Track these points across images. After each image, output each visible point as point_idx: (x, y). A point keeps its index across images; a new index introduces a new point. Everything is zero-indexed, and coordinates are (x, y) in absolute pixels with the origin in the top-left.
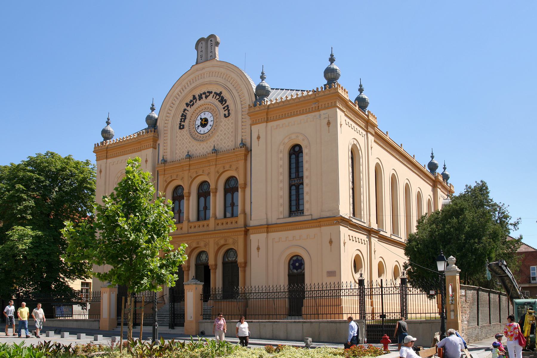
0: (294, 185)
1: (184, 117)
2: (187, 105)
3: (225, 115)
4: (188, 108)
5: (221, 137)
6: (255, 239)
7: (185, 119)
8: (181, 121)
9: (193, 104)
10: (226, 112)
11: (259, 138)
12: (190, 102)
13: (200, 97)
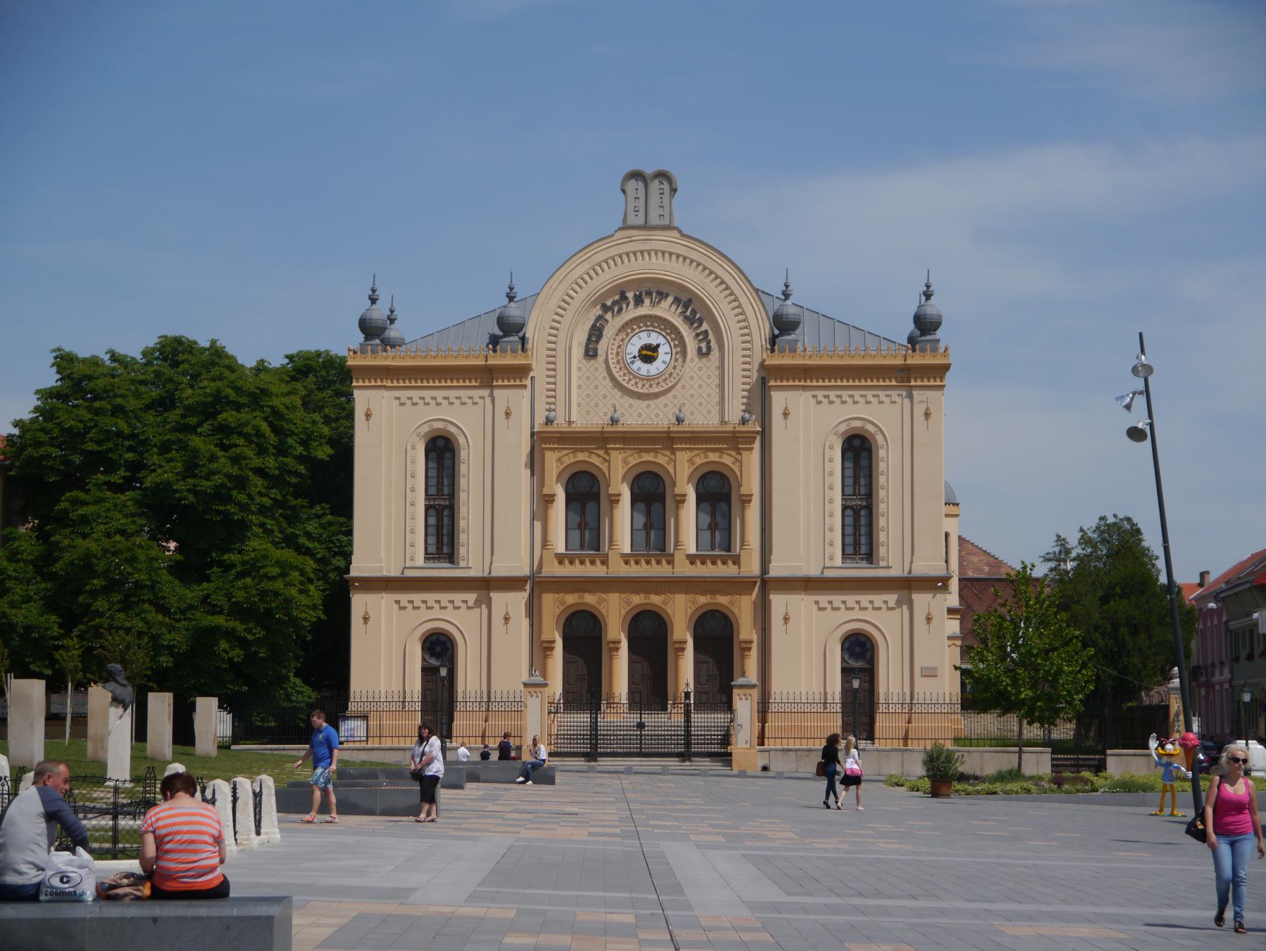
0: (850, 507)
1: (596, 333)
2: (605, 308)
3: (700, 349)
4: (608, 316)
5: (692, 391)
6: (779, 602)
7: (600, 336)
8: (589, 340)
9: (620, 310)
10: (703, 345)
11: (786, 415)
12: (614, 303)
13: (639, 301)
